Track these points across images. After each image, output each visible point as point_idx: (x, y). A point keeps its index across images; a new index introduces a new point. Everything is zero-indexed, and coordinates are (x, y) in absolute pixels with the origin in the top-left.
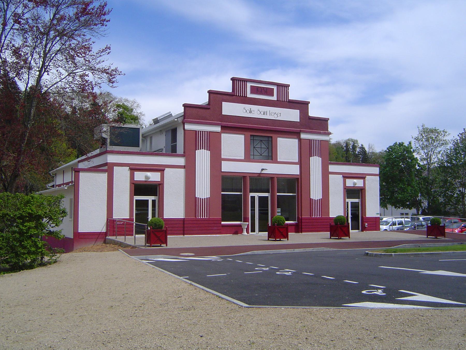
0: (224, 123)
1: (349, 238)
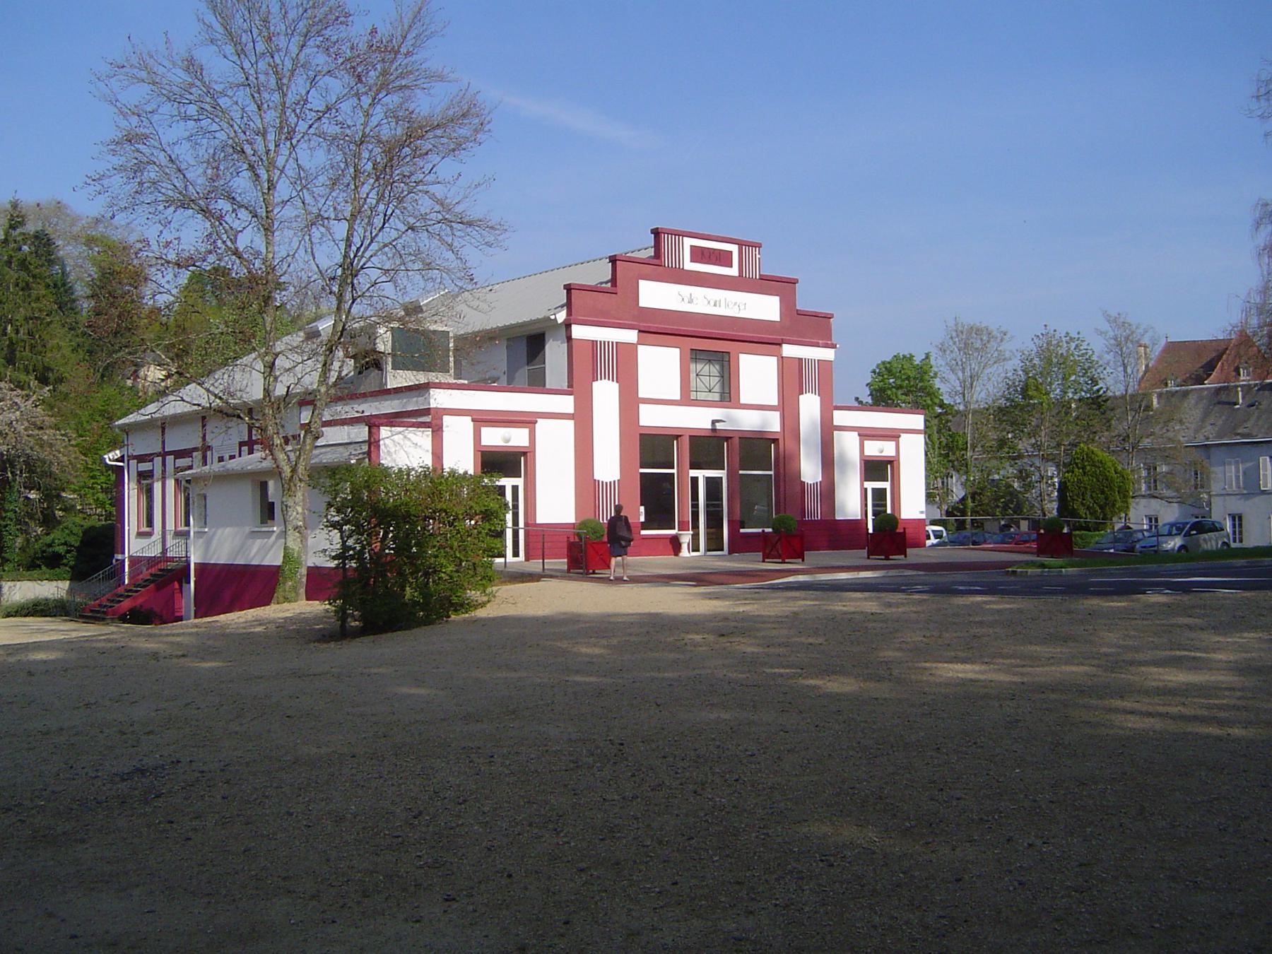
0: (644, 325)
1: (906, 556)
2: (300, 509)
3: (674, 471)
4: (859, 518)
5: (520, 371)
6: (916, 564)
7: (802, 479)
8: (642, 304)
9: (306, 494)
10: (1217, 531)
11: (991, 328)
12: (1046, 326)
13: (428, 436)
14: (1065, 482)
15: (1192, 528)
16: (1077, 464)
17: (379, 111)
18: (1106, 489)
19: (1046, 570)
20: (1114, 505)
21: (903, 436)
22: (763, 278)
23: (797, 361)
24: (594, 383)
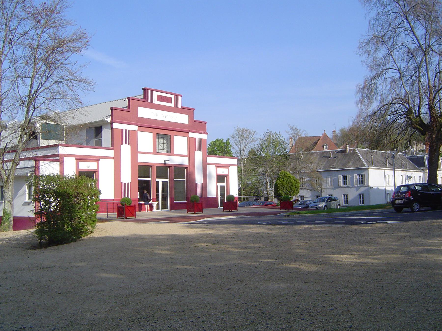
0: (140, 124)
1: (237, 210)
2: (10, 193)
3: (150, 179)
4: (216, 196)
5: (92, 140)
6: (241, 213)
7: (196, 182)
8: (139, 116)
9: (13, 187)
10: (336, 200)
11: (251, 130)
12: (268, 129)
13: (58, 165)
14: (277, 184)
15: (328, 199)
16: (281, 178)
17: (45, 35)
18: (291, 186)
19: (301, 215)
20: (294, 192)
21: (230, 166)
22: (182, 108)
23: (194, 139)
24: (121, 145)
